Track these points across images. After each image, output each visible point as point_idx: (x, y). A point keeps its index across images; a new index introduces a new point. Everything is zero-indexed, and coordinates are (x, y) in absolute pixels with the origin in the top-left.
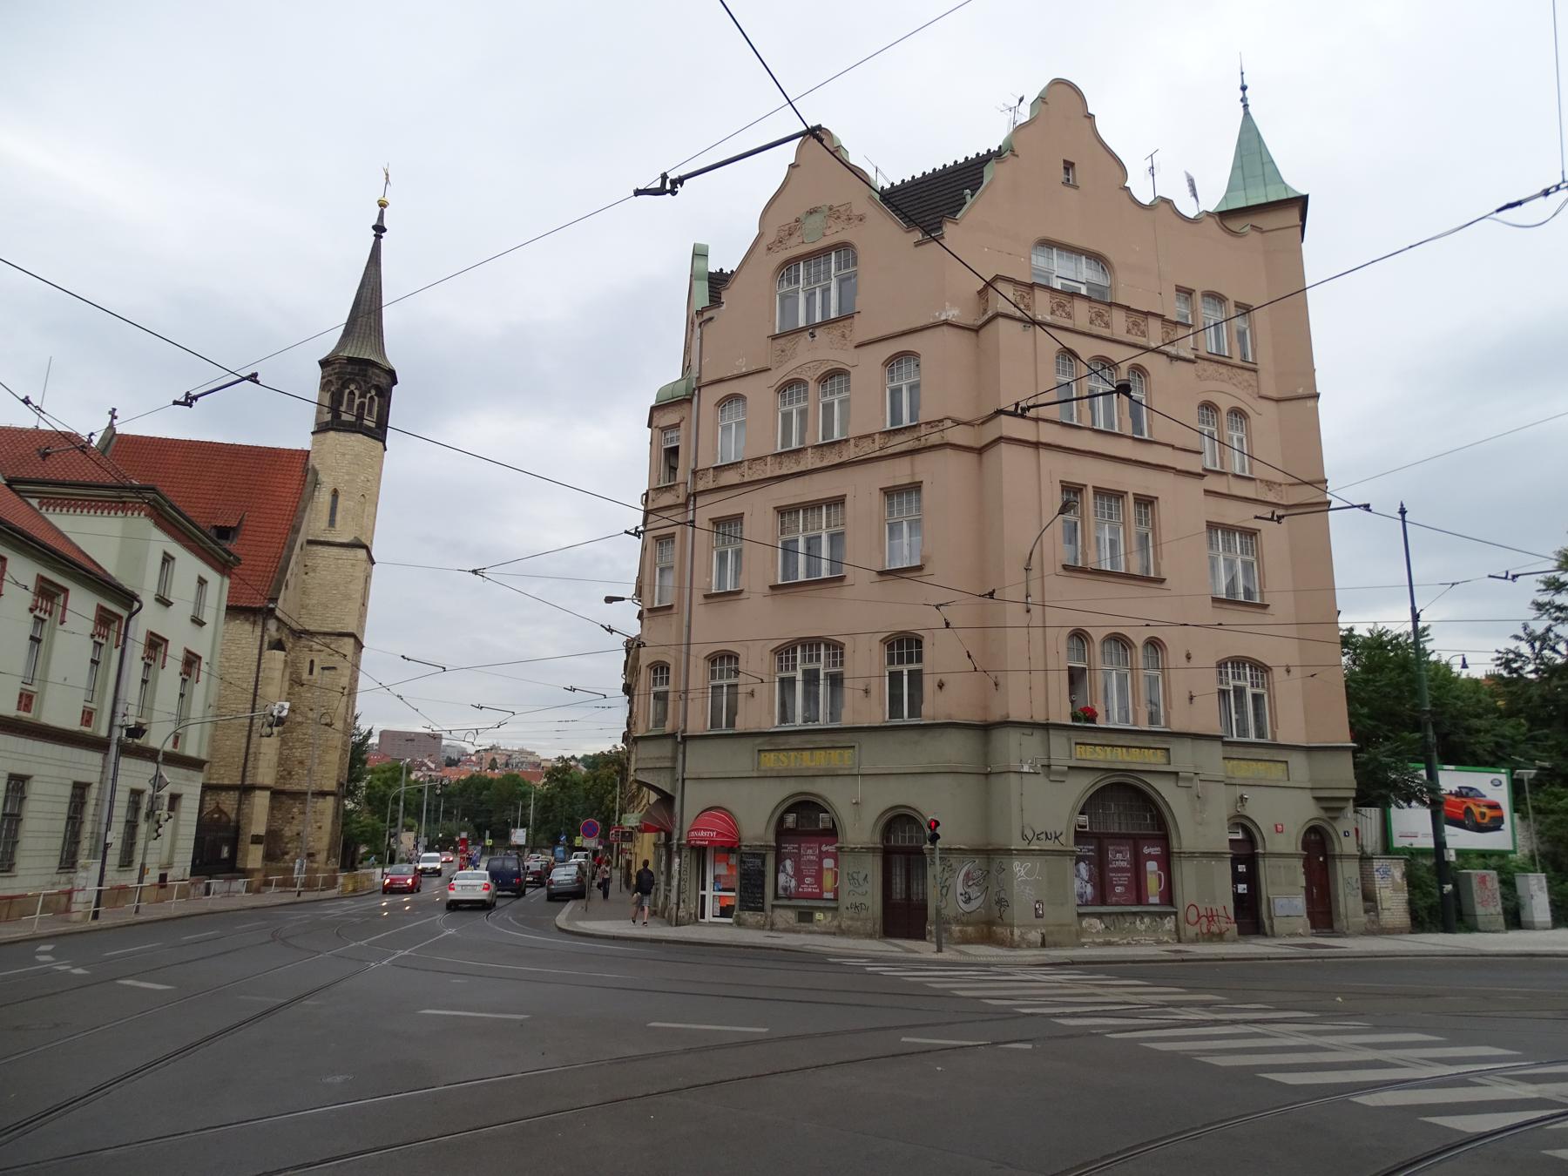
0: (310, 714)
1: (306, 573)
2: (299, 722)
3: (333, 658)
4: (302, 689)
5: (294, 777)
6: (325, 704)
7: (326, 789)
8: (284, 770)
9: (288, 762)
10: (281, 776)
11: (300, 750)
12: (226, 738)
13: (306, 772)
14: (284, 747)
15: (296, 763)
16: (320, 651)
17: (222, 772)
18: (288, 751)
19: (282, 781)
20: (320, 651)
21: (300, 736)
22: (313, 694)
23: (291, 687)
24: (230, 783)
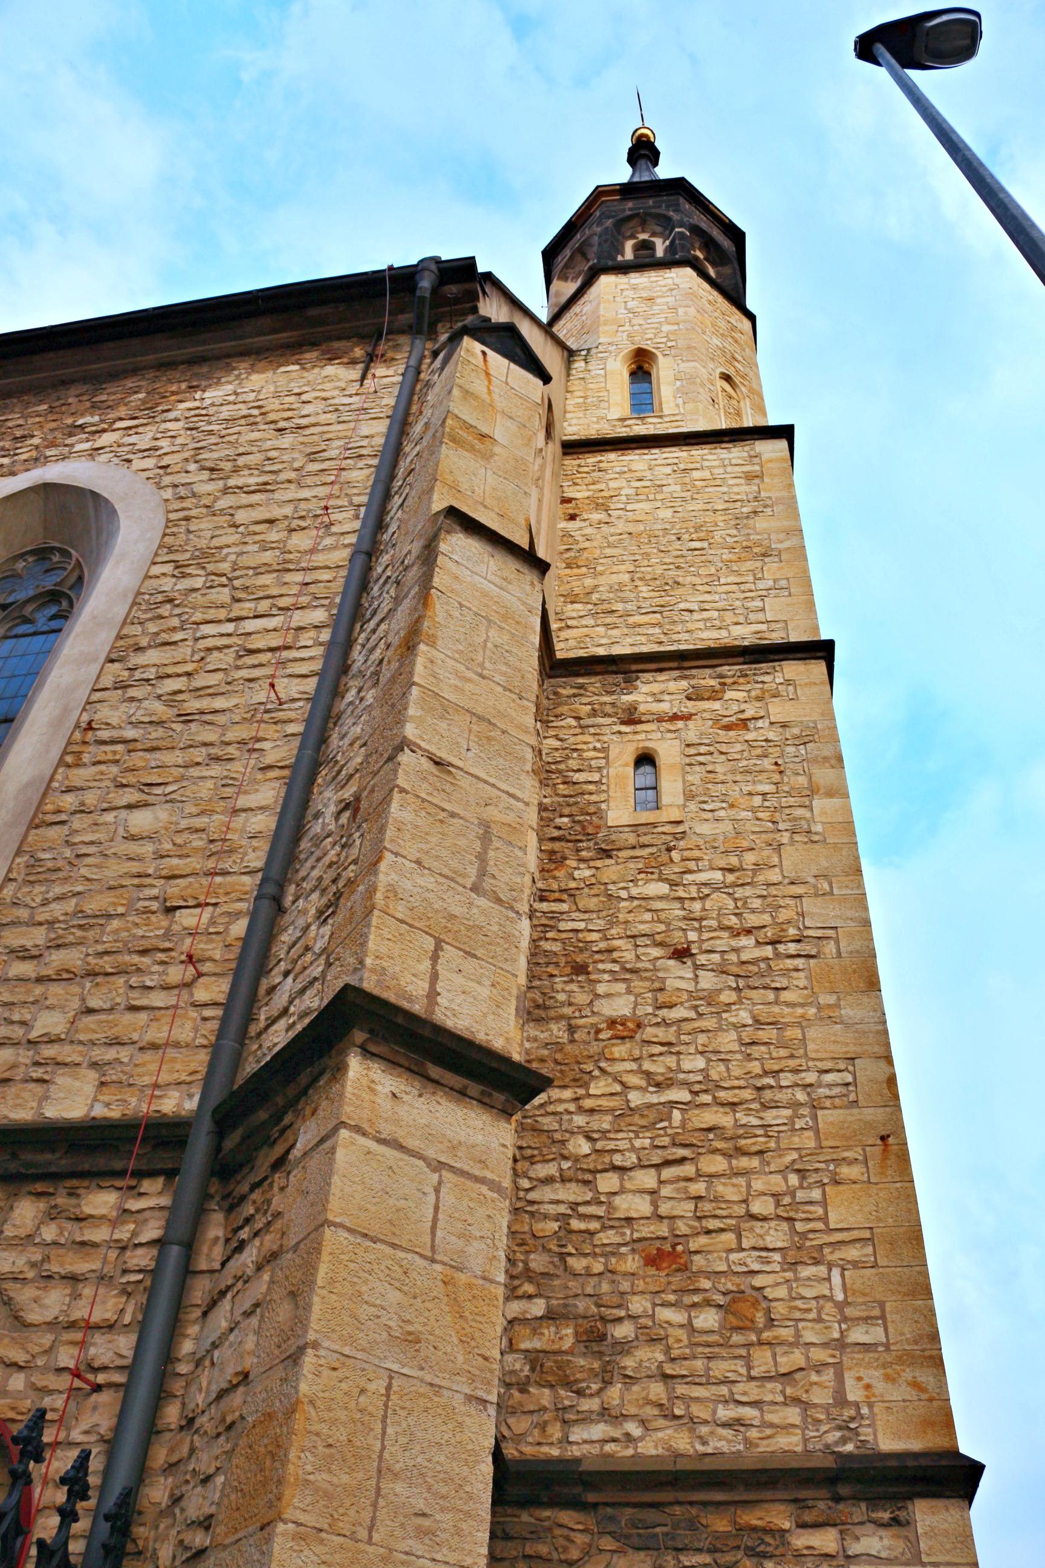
0: (678, 976)
1: (573, 517)
2: (612, 1023)
3: (750, 736)
4: (610, 870)
5: (629, 1362)
6: (753, 920)
7: (887, 1444)
8: (550, 1316)
9: (577, 1264)
10: (534, 1359)
11: (647, 1179)
12: (131, 796)
13: (708, 1319)
14: (543, 1170)
15: (631, 1263)
16: (675, 717)
17: (49, 1022)
18: (572, 1193)
19: (545, 1396)
20: (675, 717)
21: (636, 1099)
22: (673, 884)
23: (552, 860)
24: (105, 1110)
